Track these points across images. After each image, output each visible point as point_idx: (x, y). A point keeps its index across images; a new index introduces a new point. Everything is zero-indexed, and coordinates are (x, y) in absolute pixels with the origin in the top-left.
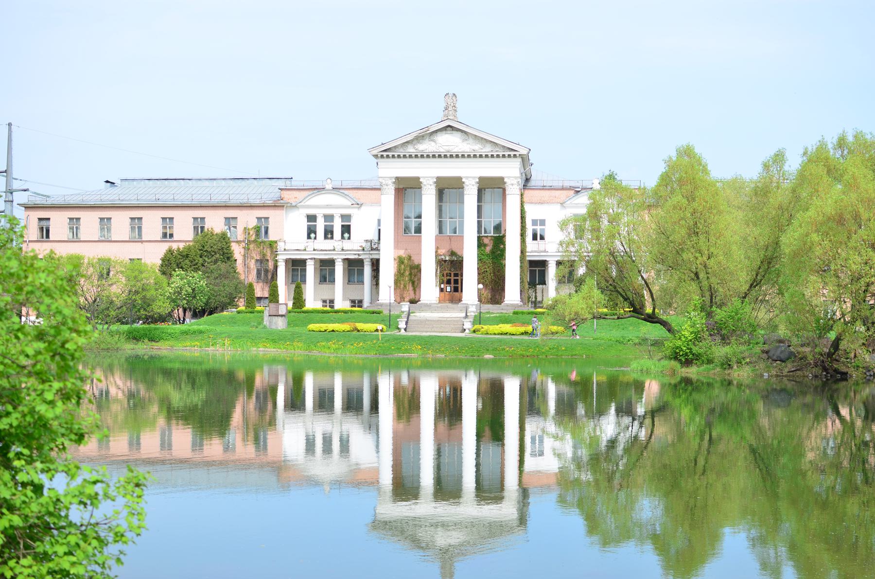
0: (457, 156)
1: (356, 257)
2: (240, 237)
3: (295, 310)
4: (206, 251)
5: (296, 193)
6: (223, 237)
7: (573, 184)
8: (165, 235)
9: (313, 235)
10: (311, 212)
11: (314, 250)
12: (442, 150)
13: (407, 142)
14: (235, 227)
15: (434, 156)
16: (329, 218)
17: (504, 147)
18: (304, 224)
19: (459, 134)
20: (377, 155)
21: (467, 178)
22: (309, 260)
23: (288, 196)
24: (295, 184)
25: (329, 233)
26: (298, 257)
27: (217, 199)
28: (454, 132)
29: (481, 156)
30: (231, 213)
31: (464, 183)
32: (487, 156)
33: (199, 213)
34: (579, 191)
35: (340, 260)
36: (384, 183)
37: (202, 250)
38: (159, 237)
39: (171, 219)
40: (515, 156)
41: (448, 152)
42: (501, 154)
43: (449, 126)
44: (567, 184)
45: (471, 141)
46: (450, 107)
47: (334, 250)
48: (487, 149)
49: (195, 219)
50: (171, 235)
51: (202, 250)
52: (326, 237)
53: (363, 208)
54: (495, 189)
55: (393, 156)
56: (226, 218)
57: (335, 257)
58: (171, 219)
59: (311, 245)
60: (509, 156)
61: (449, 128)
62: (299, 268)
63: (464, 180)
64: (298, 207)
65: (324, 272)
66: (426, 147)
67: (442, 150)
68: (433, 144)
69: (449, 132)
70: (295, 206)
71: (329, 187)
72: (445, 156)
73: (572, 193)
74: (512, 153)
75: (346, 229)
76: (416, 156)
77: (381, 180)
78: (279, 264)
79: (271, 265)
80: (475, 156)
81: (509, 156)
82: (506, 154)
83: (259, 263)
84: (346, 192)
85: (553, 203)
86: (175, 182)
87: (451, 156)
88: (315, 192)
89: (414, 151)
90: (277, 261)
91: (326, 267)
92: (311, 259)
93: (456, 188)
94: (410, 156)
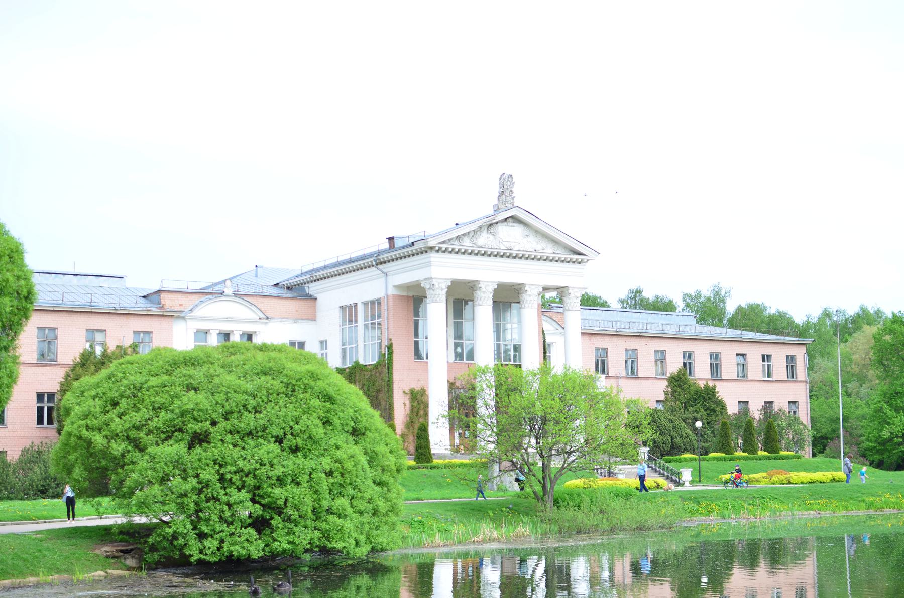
5: (182, 299)
10: (204, 326)
19: (522, 226)
20: (435, 247)
36: (437, 287)
56: (88, 330)
66: (485, 240)
68: (491, 237)
69: (511, 224)
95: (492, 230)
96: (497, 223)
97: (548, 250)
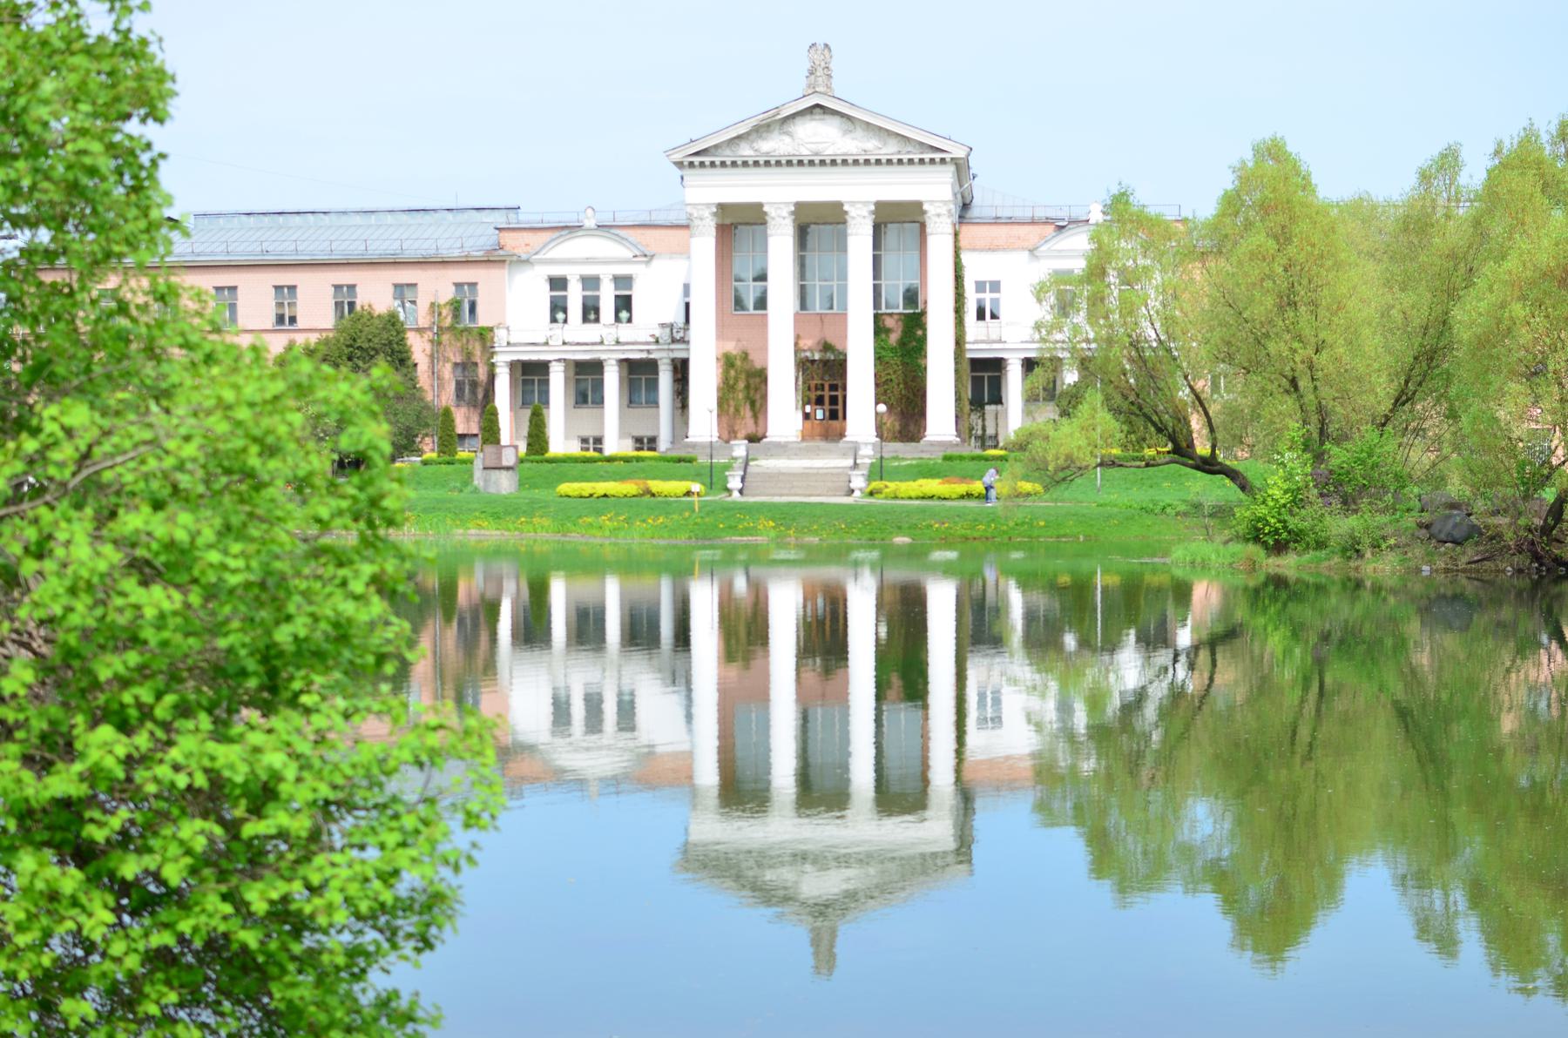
0: (834, 162)
1: (644, 355)
2: (424, 320)
3: (532, 457)
4: (360, 348)
6: (392, 320)
7: (1052, 214)
8: (280, 319)
9: (560, 316)
10: (557, 271)
11: (564, 343)
12: (806, 152)
13: (739, 137)
14: (414, 302)
15: (789, 163)
16: (591, 282)
17: (921, 144)
18: (544, 295)
19: (836, 121)
21: (853, 203)
22: (554, 363)
23: (509, 240)
24: (525, 217)
25: (591, 311)
26: (534, 357)
27: (381, 246)
28: (827, 117)
29: (878, 162)
30: (405, 276)
31: (846, 213)
32: (889, 162)
33: (345, 277)
34: (1063, 227)
35: (614, 362)
37: (351, 346)
38: (269, 322)
39: (292, 288)
40: (943, 161)
41: (817, 154)
42: (916, 157)
43: (818, 106)
44: (1040, 214)
45: (859, 133)
46: (819, 69)
47: (602, 343)
48: (890, 150)
49: (338, 287)
50: (293, 320)
51: (351, 346)
52: (585, 319)
53: (655, 262)
54: (906, 225)
55: (713, 164)
56: (396, 286)
57: (603, 357)
58: (292, 288)
59: (559, 333)
60: (932, 161)
61: (818, 110)
62: (536, 378)
63: (846, 208)
64: (532, 264)
65: (582, 386)
66: (775, 145)
67: (805, 152)
68: (787, 139)
70: (527, 261)
71: (590, 223)
72: (811, 163)
73: (1050, 229)
74: (938, 156)
75: (624, 303)
76: (756, 163)
77: (689, 209)
78: (498, 370)
79: (482, 374)
80: (867, 162)
81: (932, 161)
82: (927, 156)
83: (459, 370)
84: (622, 233)
85: (1014, 249)
86: (297, 218)
87: (822, 163)
88: (564, 233)
89: (752, 153)
90: (493, 365)
91: (586, 375)
92: (559, 360)
93: (831, 224)
94: (745, 164)
95: (786, 128)
96: (793, 116)
97: (890, 150)
